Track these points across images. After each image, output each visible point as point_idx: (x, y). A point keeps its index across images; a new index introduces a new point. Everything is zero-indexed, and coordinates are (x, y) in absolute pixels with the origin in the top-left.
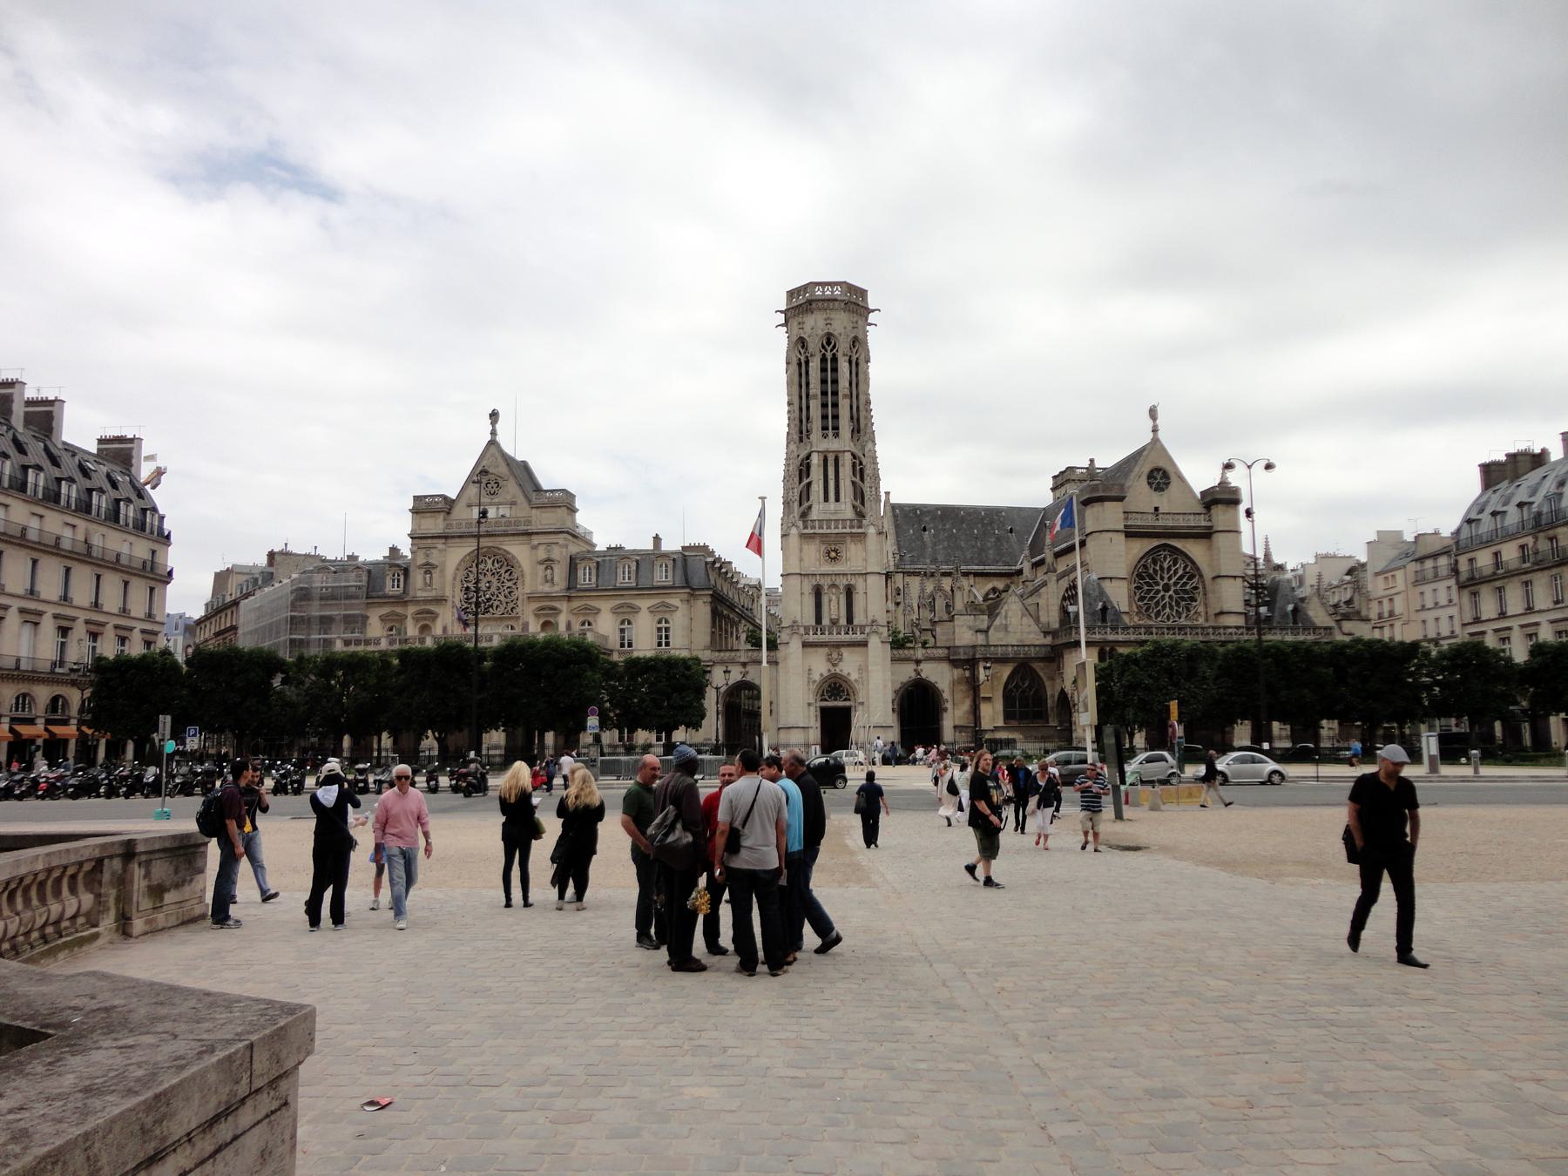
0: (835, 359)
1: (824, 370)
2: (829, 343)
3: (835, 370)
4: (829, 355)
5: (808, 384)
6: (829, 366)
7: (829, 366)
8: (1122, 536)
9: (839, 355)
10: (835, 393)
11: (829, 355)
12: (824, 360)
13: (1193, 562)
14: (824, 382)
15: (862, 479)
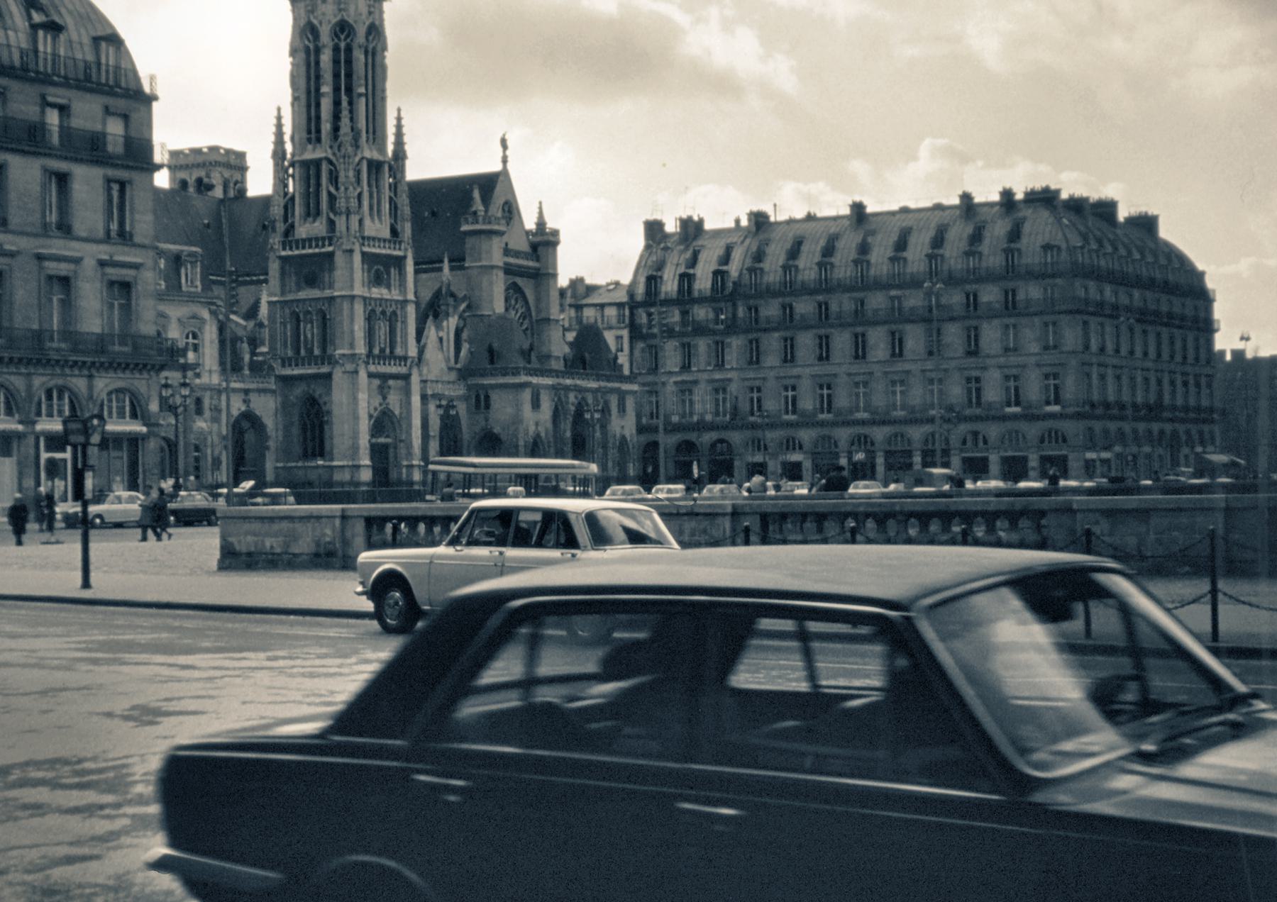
0: (349, 49)
1: (336, 62)
2: (342, 30)
3: (349, 62)
4: (343, 45)
5: (349, 75)
6: (343, 60)
7: (343, 60)
8: (501, 274)
9: (355, 46)
10: (349, 90)
11: (343, 45)
12: (336, 49)
13: (527, 302)
14: (336, 76)
15: (337, 189)
